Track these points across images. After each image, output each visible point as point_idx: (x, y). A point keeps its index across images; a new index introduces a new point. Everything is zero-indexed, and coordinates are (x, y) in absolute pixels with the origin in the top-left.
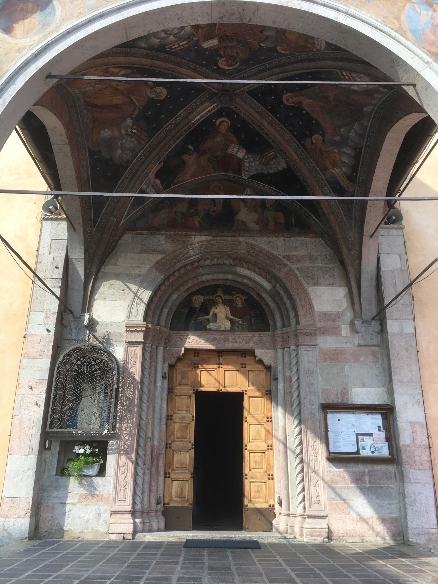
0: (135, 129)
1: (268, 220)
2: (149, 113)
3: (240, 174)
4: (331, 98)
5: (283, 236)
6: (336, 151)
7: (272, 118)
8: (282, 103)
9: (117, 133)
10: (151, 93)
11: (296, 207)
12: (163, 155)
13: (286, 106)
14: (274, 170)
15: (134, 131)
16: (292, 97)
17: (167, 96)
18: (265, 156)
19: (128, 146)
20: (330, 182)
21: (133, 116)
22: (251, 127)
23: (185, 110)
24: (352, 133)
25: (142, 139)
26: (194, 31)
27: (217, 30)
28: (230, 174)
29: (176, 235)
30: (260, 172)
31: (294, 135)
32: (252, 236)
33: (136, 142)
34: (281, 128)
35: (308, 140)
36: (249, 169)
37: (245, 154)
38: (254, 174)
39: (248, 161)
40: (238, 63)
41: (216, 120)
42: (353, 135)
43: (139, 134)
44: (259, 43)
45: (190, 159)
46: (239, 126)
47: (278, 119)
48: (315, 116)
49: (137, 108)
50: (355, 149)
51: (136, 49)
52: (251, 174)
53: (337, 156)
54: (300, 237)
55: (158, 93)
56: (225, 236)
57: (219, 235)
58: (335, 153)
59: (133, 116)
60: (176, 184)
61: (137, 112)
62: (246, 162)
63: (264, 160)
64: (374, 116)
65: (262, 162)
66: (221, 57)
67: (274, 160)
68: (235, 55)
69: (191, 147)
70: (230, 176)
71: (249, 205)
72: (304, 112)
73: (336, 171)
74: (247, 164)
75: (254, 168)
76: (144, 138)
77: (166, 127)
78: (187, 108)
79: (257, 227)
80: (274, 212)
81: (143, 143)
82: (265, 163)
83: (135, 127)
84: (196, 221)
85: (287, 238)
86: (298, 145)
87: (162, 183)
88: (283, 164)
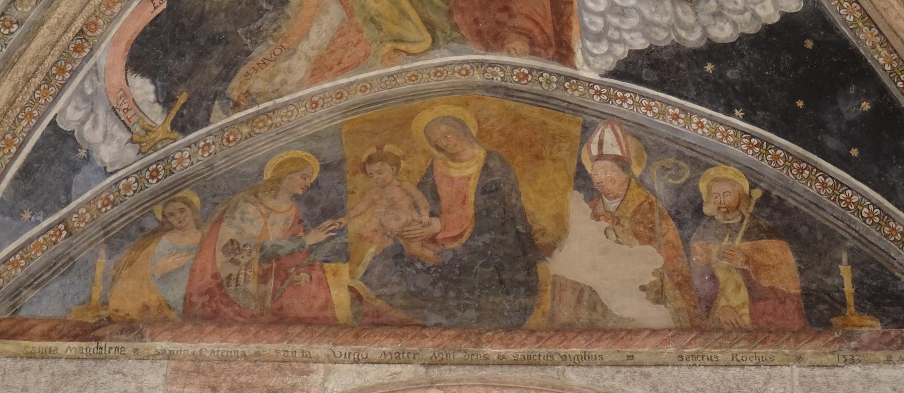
1: (713, 277)
3: (564, 54)
5: (799, 359)
11: (858, 212)
14: (735, 24)
28: (515, 59)
29: (225, 360)
30: (662, 37)
32: (631, 362)
36: (607, 25)
38: (635, 54)
52: (621, 51)
54: (889, 361)
56: (486, 362)
57: (459, 356)
60: (237, 106)
70: (515, 67)
71: (612, 205)
75: (634, 21)
79: (658, 316)
80: (747, 237)
84: (339, 289)
85: (818, 371)
87: (166, 100)
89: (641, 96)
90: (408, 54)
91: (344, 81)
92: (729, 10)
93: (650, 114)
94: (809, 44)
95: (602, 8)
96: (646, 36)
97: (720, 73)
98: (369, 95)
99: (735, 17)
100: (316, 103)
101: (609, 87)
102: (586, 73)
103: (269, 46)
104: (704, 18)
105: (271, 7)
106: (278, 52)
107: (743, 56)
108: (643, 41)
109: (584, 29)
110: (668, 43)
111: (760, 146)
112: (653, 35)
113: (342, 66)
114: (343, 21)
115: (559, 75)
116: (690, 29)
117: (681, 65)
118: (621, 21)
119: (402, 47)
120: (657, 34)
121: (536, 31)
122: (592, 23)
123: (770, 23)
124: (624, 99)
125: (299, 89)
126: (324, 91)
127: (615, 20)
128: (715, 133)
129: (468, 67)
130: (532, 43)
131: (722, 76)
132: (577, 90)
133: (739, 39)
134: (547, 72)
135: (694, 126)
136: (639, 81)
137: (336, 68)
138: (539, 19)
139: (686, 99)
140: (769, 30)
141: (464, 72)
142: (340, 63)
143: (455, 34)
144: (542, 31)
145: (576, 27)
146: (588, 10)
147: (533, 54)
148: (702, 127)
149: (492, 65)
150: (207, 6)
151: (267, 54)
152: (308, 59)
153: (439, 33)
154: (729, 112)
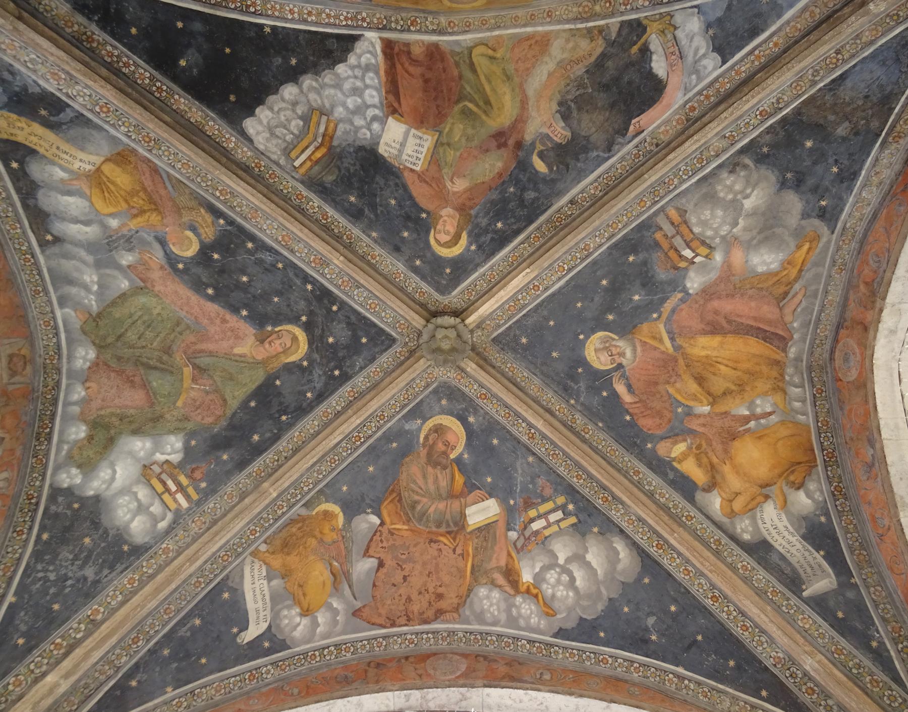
0: (686, 259)
2: (637, 297)
3: (388, 46)
4: (188, 371)
6: (114, 223)
7: (322, 275)
8: (308, 328)
9: (738, 256)
10: (622, 354)
12: (623, 158)
13: (294, 320)
14: (283, 100)
15: (688, 253)
16: (286, 351)
17: (587, 337)
18: (322, 145)
19: (719, 213)
20: (80, 119)
21: (680, 295)
22: (374, 234)
23: (546, 289)
24: (92, 281)
25: (673, 224)
26: (516, 562)
27: (468, 555)
28: (418, 39)
30: (328, 77)
31: (253, 238)
33: (693, 220)
34: (292, 251)
35: (209, 233)
36: (363, 79)
37: (380, 137)
38: (343, 60)
39: (371, 113)
40: (421, 440)
41: (467, 249)
42: (87, 278)
43: (678, 242)
44: (382, 524)
45: (544, 123)
46: (406, 234)
47: (306, 279)
48: (213, 308)
49: (665, 316)
50: (57, 240)
51: (637, 538)
52: (352, 59)
53: (99, 204)
55: (606, 348)
58: (112, 215)
59: (680, 295)
61: (668, 306)
62: (374, 106)
63: (322, 129)
64: (57, 334)
65: (324, 118)
66: (458, 461)
67: (289, 137)
68: (430, 469)
69: (540, 166)
70: (419, 31)
72: (244, 313)
73: (84, 161)
74: (373, 96)
75: (347, 86)
76: (668, 229)
77: (600, 246)
78: (539, 296)
81: (673, 213)
82: (315, 119)
83: (683, 264)
86: (232, 208)
88: (258, 133)
89: (335, 25)
90: (487, 45)
91: (529, 29)
92: (288, 109)
93: (327, 10)
94: (232, 98)
95: (367, 92)
96: (337, 75)
97: (286, 60)
98: (514, 13)
99: (284, 105)
100: (549, 16)
101: (358, 26)
102: (371, 35)
103: (573, 73)
104: (303, 99)
105: (569, 103)
106: (569, 67)
107: (273, 77)
108: (339, 71)
109: (377, 73)
110: (323, 74)
111: (248, 7)
112: (333, 77)
113: (529, 42)
114: (526, 81)
115: (390, 29)
116: (311, 89)
117: (311, 58)
118: (354, 84)
119: (490, 52)
120: (331, 79)
121: (407, 65)
122: (372, 79)
123: (261, 107)
124: (346, 19)
125: (559, 31)
126: (542, 24)
127: (359, 84)
128: (281, 8)
129: (450, 30)
130: (409, 53)
131: (284, 58)
132: (378, 19)
133: (278, 90)
134: (399, 30)
135: (296, 10)
136: (338, 37)
137: (533, 41)
138: (406, 75)
139: (305, 31)
140: (260, 101)
141: (452, 24)
142: (531, 45)
143: (457, 58)
144: (402, 65)
145: (382, 73)
146: (376, 89)
147: (407, 45)
148: (290, 10)
149: (434, 32)
150: (607, 114)
151: (576, 67)
152: (550, 55)
153: (468, 61)
154: (274, 28)
